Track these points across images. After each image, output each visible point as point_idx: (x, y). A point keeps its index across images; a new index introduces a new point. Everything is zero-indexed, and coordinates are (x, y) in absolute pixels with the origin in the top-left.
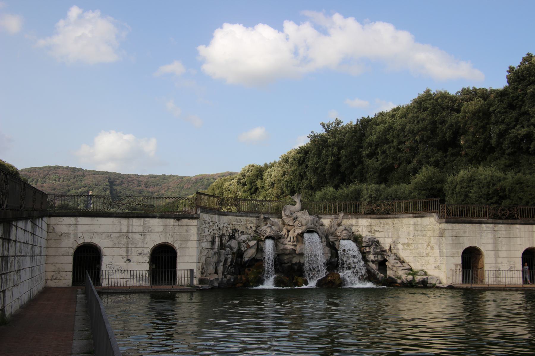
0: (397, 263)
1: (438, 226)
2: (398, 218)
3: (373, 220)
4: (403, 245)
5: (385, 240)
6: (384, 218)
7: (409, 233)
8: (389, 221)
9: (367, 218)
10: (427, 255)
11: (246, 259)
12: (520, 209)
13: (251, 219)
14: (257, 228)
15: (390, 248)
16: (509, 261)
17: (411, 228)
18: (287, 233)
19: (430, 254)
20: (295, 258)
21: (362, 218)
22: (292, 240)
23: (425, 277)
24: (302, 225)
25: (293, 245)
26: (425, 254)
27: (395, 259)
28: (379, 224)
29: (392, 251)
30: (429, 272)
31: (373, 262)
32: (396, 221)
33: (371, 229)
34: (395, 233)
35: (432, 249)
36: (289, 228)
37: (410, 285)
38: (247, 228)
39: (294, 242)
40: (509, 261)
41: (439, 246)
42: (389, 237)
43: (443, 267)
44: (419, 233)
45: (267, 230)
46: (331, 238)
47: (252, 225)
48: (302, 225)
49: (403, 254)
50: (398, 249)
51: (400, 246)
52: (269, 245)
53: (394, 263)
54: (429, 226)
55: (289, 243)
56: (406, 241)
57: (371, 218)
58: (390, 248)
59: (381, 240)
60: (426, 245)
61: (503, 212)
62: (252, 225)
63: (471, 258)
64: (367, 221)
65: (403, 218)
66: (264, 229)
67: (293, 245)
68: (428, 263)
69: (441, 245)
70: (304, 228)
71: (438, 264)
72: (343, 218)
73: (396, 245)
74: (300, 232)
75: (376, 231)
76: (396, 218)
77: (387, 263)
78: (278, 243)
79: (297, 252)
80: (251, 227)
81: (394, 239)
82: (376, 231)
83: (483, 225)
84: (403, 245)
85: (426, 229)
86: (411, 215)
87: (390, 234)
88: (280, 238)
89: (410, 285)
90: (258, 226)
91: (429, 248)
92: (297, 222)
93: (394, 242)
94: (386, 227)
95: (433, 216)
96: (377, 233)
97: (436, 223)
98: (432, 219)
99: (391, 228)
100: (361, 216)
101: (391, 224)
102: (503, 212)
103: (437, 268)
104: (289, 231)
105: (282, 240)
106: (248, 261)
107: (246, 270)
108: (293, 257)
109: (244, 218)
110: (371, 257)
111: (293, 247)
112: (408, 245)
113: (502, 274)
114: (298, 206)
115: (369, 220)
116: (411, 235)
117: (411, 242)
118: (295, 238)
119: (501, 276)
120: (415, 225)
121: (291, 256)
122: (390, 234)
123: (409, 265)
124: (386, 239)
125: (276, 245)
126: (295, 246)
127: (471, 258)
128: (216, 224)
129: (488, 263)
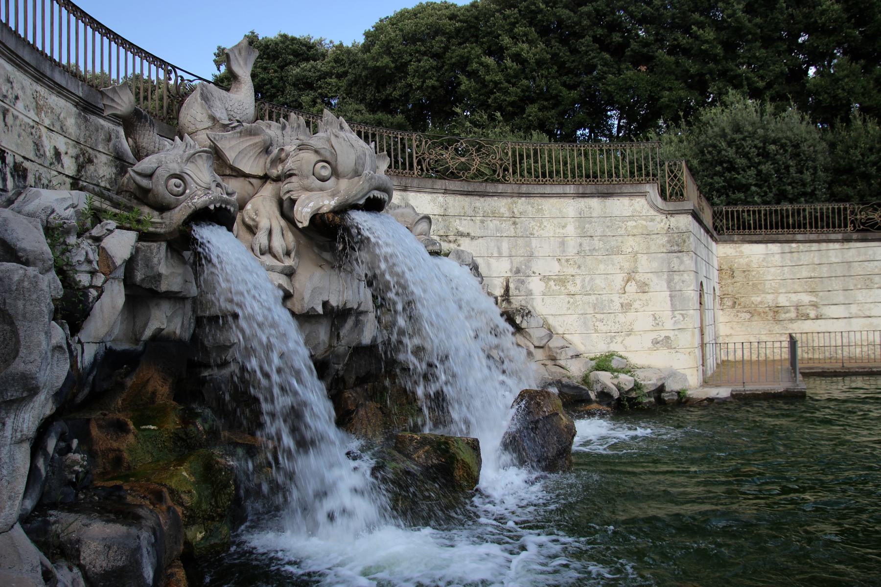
1: (661, 222)
2: (528, 195)
3: (450, 199)
4: (546, 279)
5: (489, 265)
7: (563, 244)
8: (501, 205)
9: (434, 191)
10: (626, 307)
14: (80, 167)
15: (507, 289)
17: (571, 230)
19: (636, 305)
24: (335, 173)
26: (617, 306)
28: (470, 212)
29: (513, 300)
32: (521, 204)
33: (448, 228)
34: (520, 242)
35: (643, 288)
41: (670, 281)
42: (500, 256)
44: (597, 244)
50: (530, 293)
51: (535, 285)
53: (541, 339)
54: (629, 224)
56: (554, 268)
57: (446, 192)
58: (507, 289)
60: (619, 280)
62: (61, 143)
64: (434, 200)
65: (543, 195)
68: (630, 332)
69: (677, 278)
71: (663, 334)
73: (523, 282)
74: (328, 203)
75: (462, 235)
76: (520, 195)
80: (57, 154)
81: (517, 261)
82: (462, 235)
84: (546, 279)
87: (505, 246)
91: (632, 287)
93: (518, 271)
94: (492, 224)
95: (644, 194)
97: (652, 212)
98: (640, 204)
99: (507, 228)
100: (416, 182)
101: (507, 214)
103: (666, 343)
106: (95, 363)
112: (562, 281)
115: (440, 198)
116: (571, 250)
117: (571, 270)
120: (582, 219)
122: (505, 246)
124: (492, 261)
126: (290, 273)
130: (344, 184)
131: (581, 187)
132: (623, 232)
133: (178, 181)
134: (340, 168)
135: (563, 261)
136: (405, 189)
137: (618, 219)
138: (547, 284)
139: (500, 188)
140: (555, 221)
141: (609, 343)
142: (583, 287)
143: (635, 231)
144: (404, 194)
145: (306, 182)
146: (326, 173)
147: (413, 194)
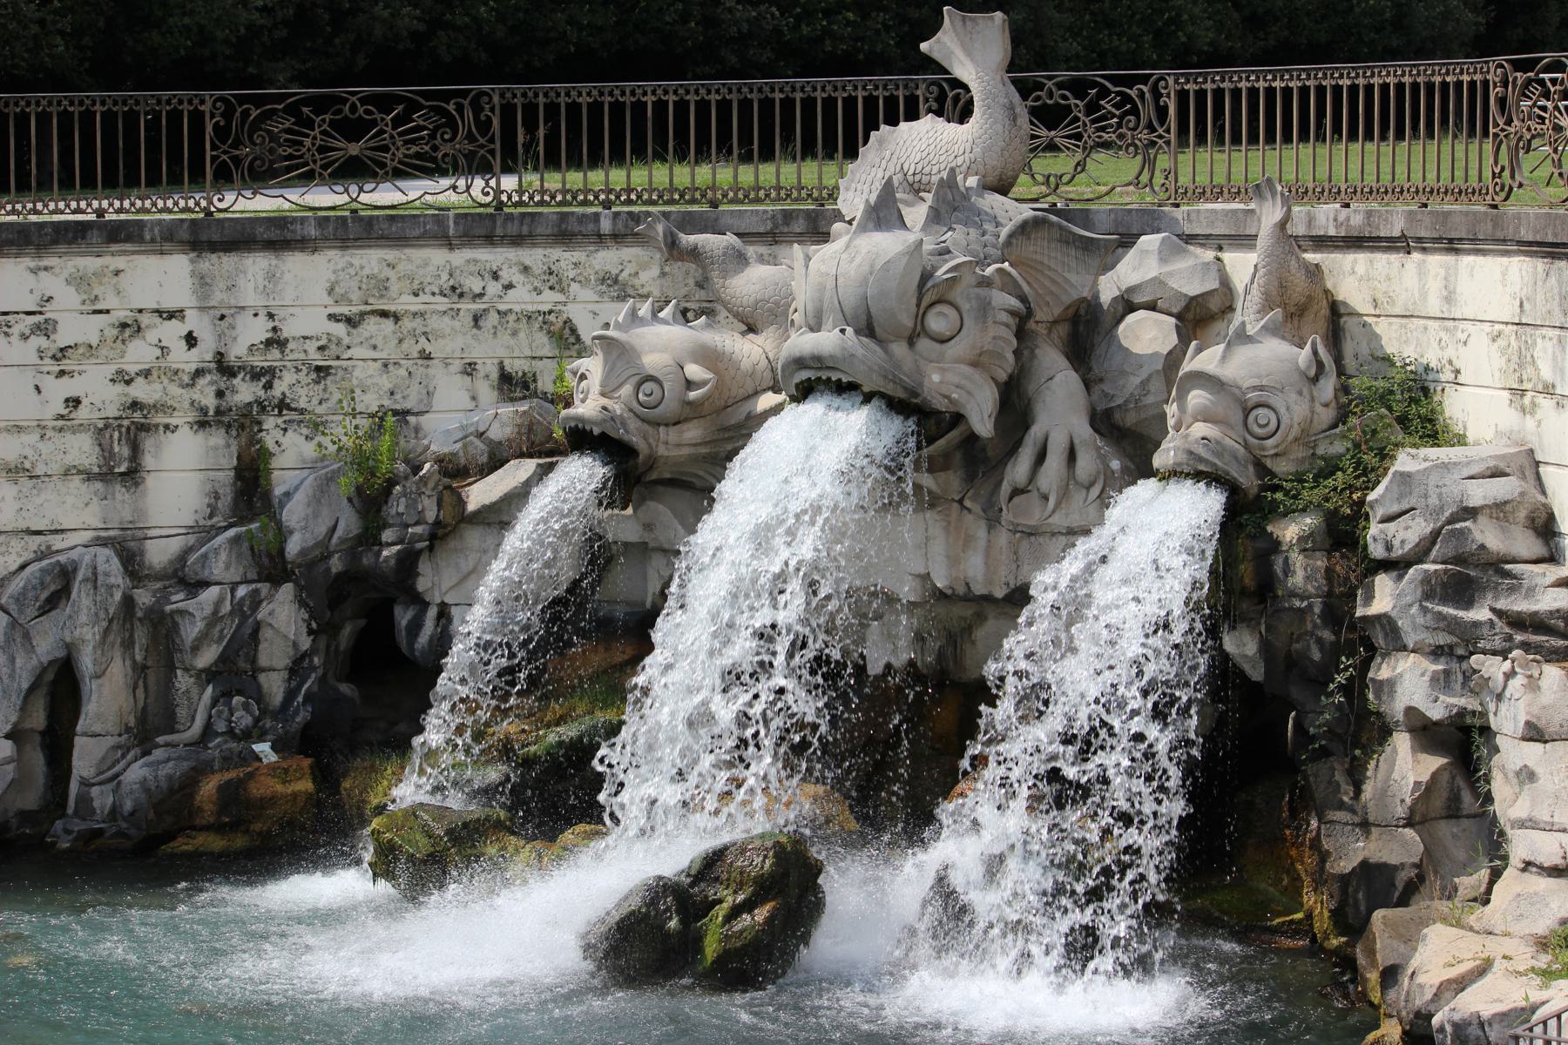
13: (608, 259)
75: (1548, 390)
82: (1548, 390)
109: (535, 256)
128: (172, 332)
136: (1452, 246)
144: (1450, 259)
147: (1471, 258)
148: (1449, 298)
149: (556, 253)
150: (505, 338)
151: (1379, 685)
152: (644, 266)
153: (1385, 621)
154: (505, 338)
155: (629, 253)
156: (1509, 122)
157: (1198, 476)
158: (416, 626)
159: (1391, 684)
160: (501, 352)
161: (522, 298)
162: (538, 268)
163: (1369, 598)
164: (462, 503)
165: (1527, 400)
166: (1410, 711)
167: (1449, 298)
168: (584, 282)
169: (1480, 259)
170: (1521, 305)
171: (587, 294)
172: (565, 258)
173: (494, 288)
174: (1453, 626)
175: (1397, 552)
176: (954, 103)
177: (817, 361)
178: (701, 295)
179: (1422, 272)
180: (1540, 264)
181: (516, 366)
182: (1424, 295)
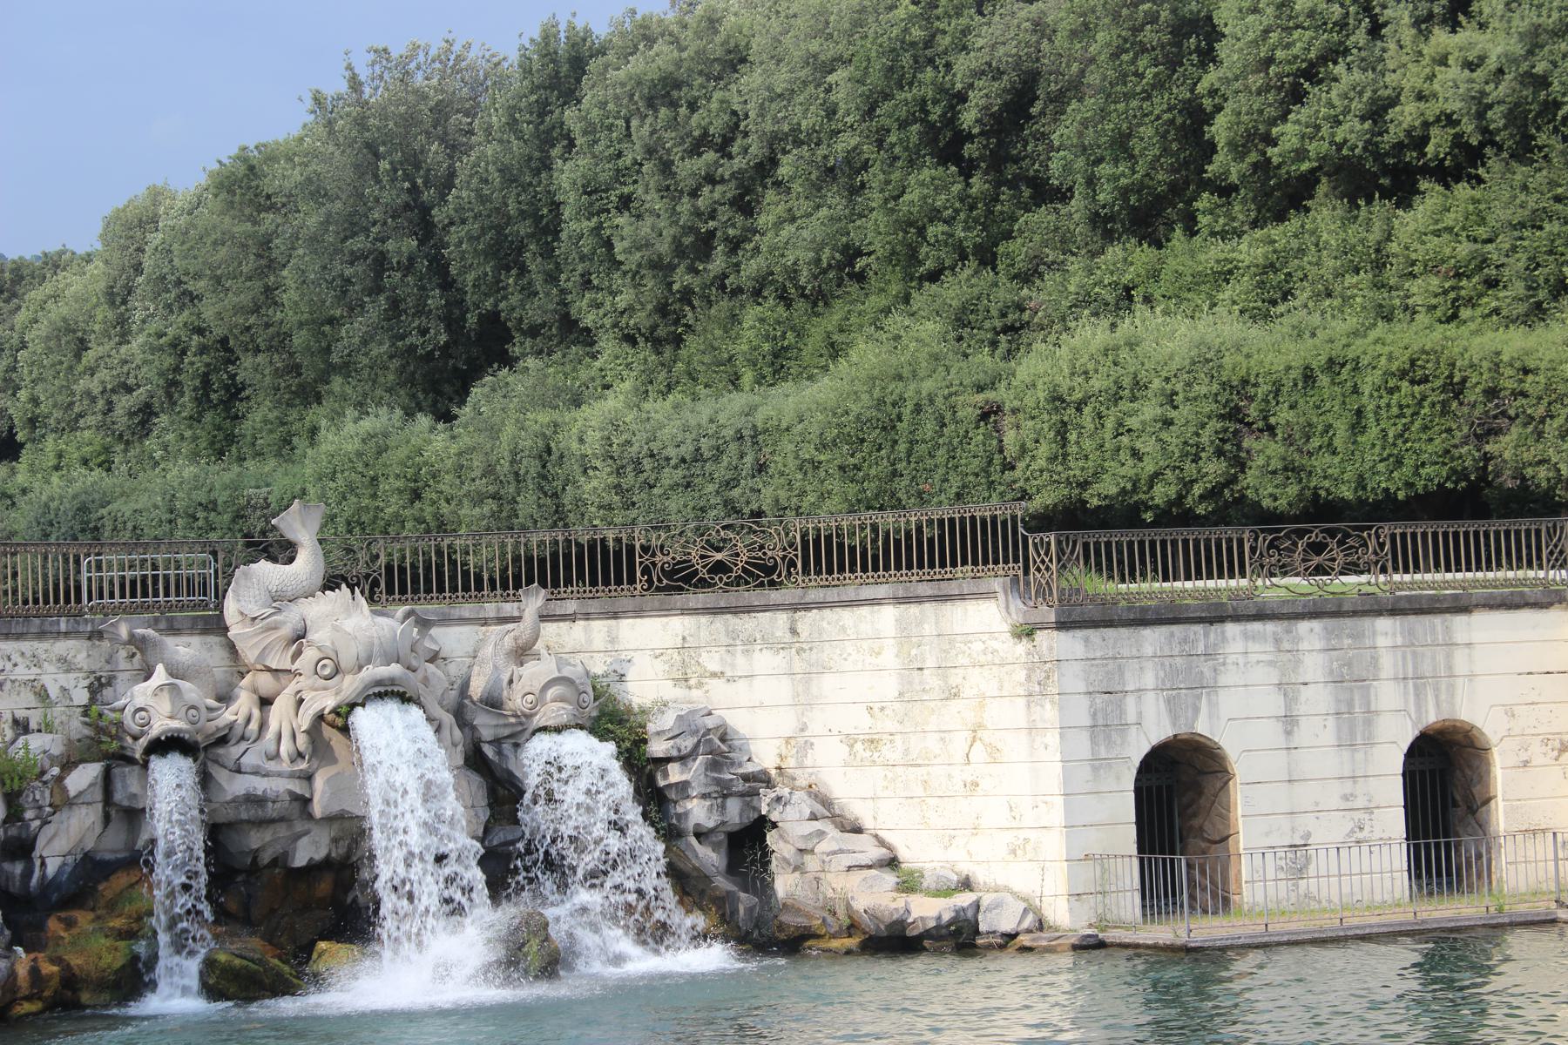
0: (821, 834)
6: (750, 609)
9: (665, 611)
11: (52, 867)
12: (1393, 537)
13: (62, 647)
16: (1346, 798)
18: (256, 713)
20: (304, 840)
21: (639, 613)
22: (286, 748)
23: (964, 899)
25: (292, 776)
27: (814, 817)
30: (980, 876)
31: (700, 835)
36: (265, 682)
37: (894, 942)
38: (42, 695)
39: (301, 755)
40: (1346, 798)
43: (1055, 846)
45: (151, 704)
46: (486, 726)
47: (68, 680)
48: (337, 671)
49: (849, 792)
52: (169, 788)
55: (271, 766)
57: (685, 611)
59: (739, 722)
60: (960, 741)
61: (1316, 560)
63: (1177, 797)
66: (139, 702)
67: (292, 776)
70: (350, 685)
72: (545, 617)
77: (771, 838)
78: (215, 771)
79: (318, 809)
83: (1231, 628)
85: (962, 660)
86: (882, 591)
88: (223, 741)
89: (894, 942)
90: (98, 686)
91: (978, 753)
92: (310, 655)
95: (989, 595)
96: (714, 683)
102: (1316, 560)
104: (265, 702)
105: (234, 751)
107: (53, 924)
108: (299, 836)
109: (26, 646)
110: (697, 812)
111: (298, 787)
112: (872, 742)
113: (1321, 863)
114: (306, 565)
118: (302, 741)
119: (1312, 870)
121: (282, 831)
123: (882, 843)
125: (205, 780)
126: (308, 778)
127: (1177, 797)
129: (1256, 816)
130: (348, 678)
131: (900, 586)
132: (966, 661)
133: (143, 713)
134: (343, 665)
135: (876, 709)
136: (615, 615)
137: (959, 638)
138: (851, 746)
139: (774, 596)
140: (865, 644)
141: (946, 848)
142: (907, 751)
143: (983, 659)
144: (612, 622)
145: (310, 682)
146: (327, 672)
148: (613, 641)
149: (36, 644)
150: (14, 696)
151: (679, 816)
152: (79, 651)
153: (683, 787)
154: (14, 696)
155: (71, 643)
156: (654, 555)
157: (582, 728)
158: (28, 873)
159: (686, 814)
160: (13, 706)
161: (22, 672)
162: (28, 654)
163: (666, 775)
164: (65, 790)
165: (692, 682)
166: (697, 825)
167: (613, 641)
168: (50, 662)
169: (638, 620)
170: (684, 638)
171: (52, 669)
172: (41, 647)
173: (9, 666)
174: (718, 782)
175: (684, 752)
176: (284, 551)
177: (392, 681)
178: (108, 667)
179: (586, 629)
180: (704, 619)
181: (20, 714)
182: (590, 641)
